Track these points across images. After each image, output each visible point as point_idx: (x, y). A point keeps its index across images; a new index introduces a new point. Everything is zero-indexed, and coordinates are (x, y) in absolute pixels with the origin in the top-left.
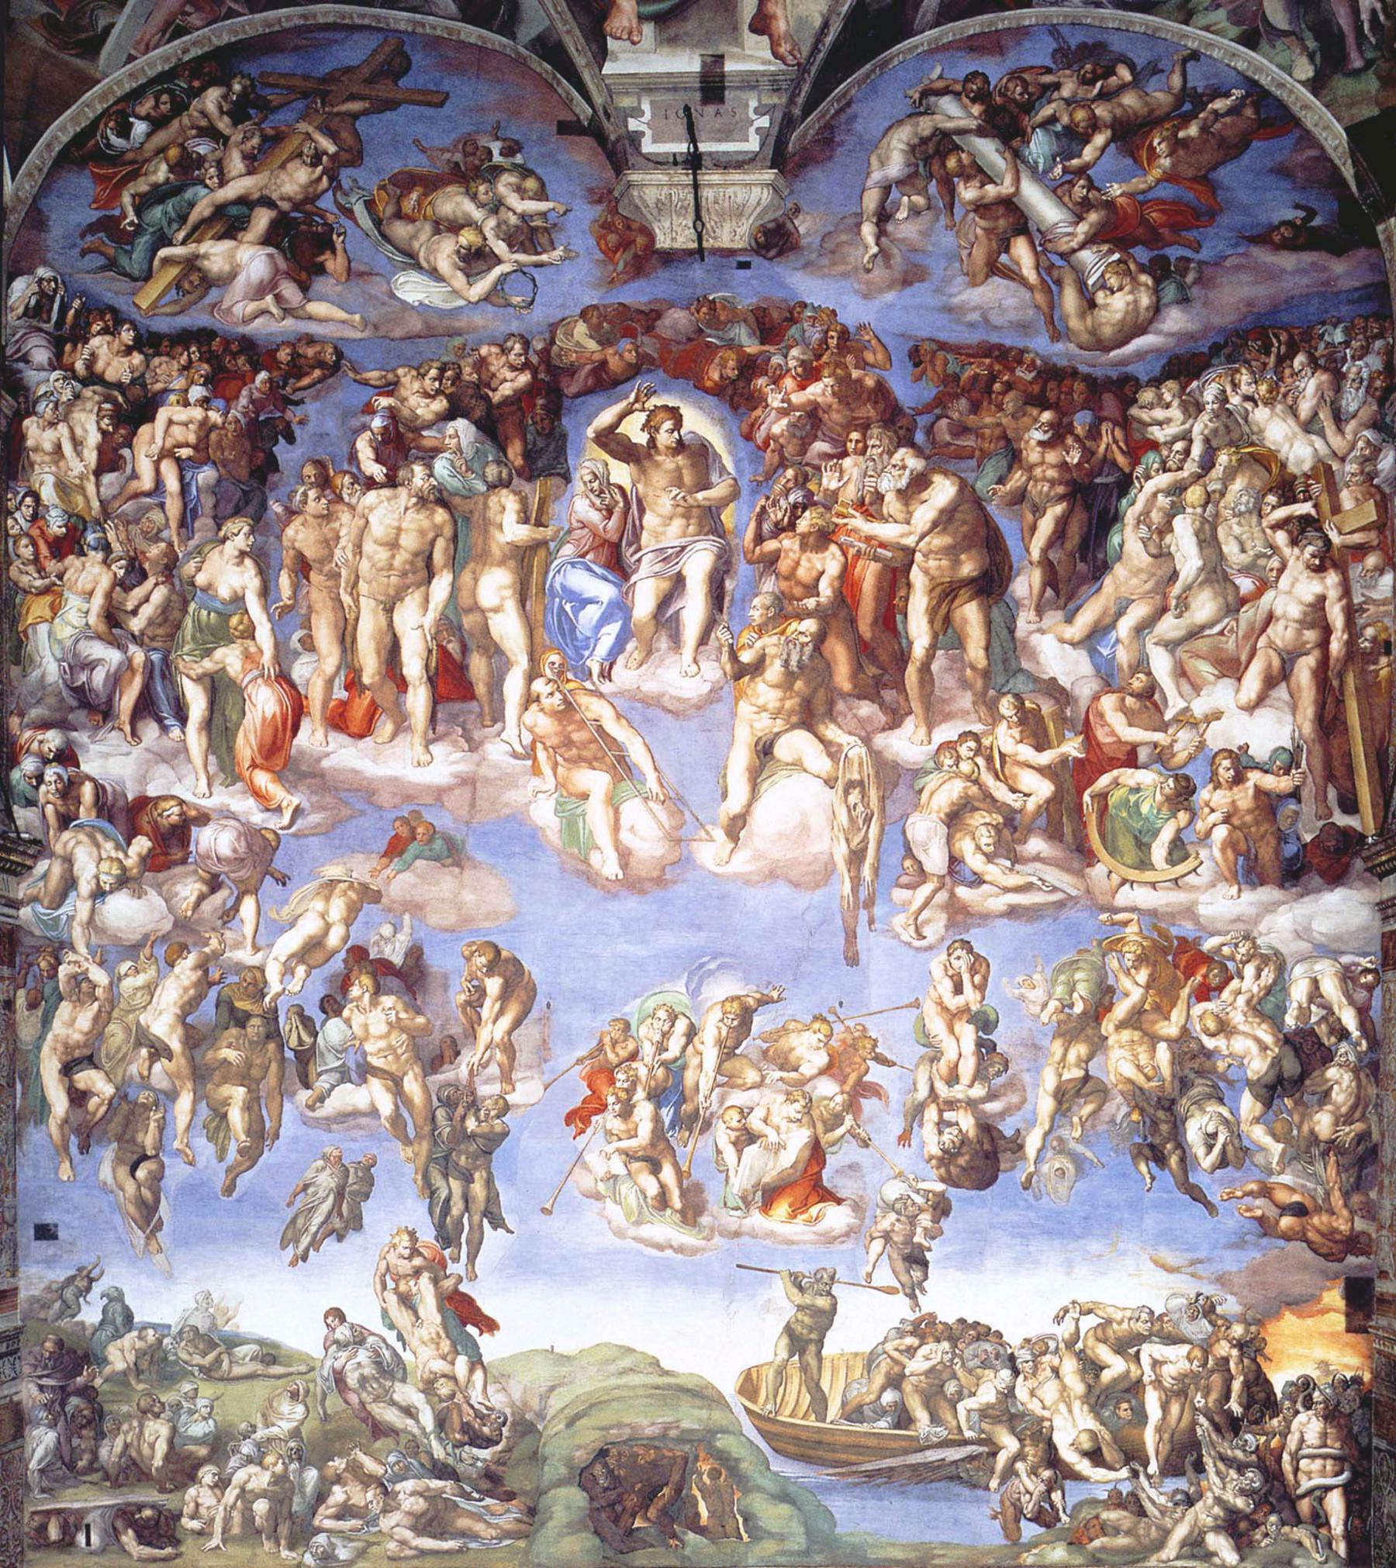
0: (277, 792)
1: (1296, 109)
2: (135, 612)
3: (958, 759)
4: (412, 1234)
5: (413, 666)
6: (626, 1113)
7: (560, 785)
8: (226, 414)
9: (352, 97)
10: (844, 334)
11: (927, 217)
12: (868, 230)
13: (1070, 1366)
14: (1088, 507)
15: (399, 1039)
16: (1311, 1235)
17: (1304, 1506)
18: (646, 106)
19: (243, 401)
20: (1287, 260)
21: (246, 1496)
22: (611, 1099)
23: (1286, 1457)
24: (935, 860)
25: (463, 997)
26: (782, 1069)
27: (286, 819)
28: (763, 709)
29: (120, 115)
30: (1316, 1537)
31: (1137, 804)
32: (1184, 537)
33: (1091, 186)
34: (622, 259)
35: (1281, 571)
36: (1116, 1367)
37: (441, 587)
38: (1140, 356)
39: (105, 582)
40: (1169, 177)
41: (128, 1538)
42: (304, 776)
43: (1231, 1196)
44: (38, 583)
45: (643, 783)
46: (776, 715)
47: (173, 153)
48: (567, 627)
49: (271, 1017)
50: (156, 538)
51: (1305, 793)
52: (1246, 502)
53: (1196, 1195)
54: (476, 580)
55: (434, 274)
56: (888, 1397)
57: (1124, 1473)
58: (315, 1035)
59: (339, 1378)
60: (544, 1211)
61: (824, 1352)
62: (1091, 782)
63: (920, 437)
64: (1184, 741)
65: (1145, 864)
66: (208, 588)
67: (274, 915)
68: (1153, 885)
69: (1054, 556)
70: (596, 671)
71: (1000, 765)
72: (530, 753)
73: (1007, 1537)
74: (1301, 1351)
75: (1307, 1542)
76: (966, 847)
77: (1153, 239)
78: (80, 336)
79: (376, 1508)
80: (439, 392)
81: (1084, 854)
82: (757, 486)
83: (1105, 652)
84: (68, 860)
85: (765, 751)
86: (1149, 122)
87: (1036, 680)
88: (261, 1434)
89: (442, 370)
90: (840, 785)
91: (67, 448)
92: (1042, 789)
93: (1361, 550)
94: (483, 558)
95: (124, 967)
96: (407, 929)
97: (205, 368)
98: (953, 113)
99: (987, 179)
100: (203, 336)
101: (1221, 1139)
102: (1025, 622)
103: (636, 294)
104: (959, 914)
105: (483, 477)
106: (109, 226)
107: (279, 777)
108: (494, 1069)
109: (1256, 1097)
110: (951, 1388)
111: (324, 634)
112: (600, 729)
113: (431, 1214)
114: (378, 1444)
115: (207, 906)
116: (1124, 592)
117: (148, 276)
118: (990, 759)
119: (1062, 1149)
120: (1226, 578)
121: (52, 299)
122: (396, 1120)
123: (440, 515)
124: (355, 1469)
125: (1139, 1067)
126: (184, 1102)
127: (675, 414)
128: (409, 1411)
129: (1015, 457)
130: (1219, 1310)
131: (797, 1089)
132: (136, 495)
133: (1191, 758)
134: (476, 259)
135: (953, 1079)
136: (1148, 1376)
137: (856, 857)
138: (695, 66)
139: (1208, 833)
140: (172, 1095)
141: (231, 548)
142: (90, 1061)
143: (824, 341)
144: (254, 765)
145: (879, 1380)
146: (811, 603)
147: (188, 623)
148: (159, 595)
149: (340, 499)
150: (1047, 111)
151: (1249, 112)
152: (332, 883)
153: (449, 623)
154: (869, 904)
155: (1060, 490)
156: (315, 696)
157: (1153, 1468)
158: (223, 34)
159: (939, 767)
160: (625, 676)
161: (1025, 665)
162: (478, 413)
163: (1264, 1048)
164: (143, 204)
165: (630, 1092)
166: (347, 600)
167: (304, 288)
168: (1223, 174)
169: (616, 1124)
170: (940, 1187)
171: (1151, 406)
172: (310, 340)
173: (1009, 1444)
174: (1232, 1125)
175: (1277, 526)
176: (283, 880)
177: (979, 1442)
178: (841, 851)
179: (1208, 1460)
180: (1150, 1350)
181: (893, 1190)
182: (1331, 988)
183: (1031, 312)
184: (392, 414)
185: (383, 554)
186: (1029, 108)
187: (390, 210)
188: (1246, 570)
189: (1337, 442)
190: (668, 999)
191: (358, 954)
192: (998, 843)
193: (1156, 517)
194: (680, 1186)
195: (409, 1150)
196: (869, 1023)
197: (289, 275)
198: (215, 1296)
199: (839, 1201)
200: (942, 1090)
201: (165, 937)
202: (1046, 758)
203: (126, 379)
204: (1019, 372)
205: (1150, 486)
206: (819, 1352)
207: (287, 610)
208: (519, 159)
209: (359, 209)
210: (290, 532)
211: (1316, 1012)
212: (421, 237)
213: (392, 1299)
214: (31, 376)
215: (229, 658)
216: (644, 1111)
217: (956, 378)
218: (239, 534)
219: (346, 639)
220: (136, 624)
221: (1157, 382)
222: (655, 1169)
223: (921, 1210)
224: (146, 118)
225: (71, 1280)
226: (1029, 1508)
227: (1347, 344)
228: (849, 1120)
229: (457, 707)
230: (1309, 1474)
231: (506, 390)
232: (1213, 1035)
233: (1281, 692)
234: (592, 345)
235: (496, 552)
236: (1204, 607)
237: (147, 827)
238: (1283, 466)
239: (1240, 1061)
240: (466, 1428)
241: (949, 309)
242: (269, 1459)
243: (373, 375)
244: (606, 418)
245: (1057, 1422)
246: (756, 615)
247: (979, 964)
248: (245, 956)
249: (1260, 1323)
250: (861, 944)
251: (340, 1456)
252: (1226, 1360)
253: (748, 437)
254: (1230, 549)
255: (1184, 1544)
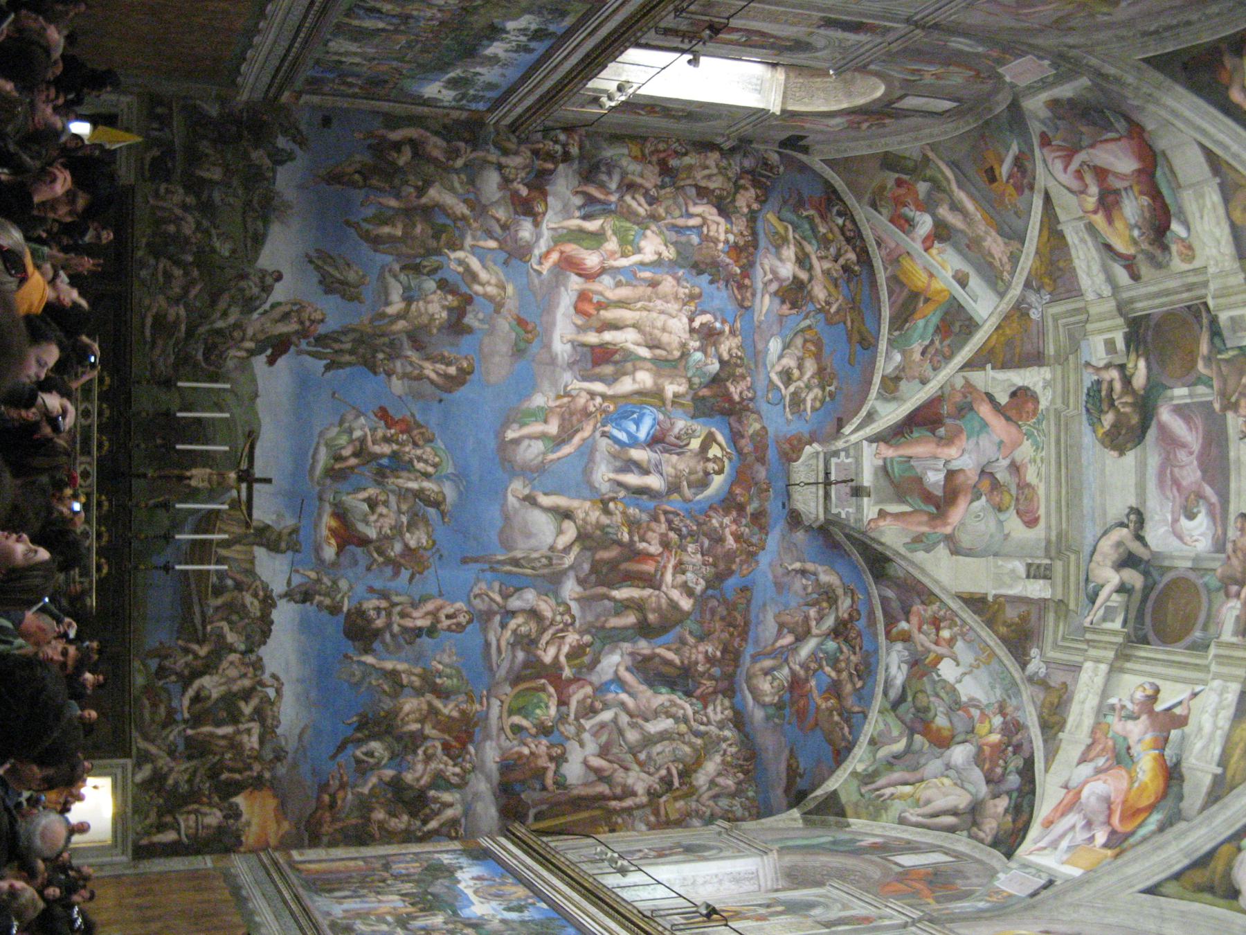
0: (547, 265)
1: (844, 765)
2: (633, 198)
3: (562, 614)
4: (322, 321)
5: (608, 336)
6: (387, 440)
7: (551, 409)
8: (723, 252)
9: (853, 321)
10: (753, 555)
11: (801, 593)
12: (797, 565)
13: (247, 683)
14: (678, 676)
15: (425, 320)
16: (320, 812)
17: (168, 819)
18: (849, 460)
19: (728, 260)
20: (783, 767)
21: (177, 220)
22: (393, 431)
23: (195, 806)
24: (515, 603)
25: (446, 354)
26: (409, 522)
27: (536, 267)
28: (587, 514)
29: (846, 213)
30: (151, 826)
31: (539, 707)
32: (665, 724)
33: (815, 671)
34: (787, 447)
35: (649, 773)
36: (247, 709)
37: (644, 352)
38: (744, 698)
39: (648, 185)
40: (818, 708)
41: (156, 152)
42: (557, 276)
43: (340, 767)
44: (647, 151)
45: (553, 452)
46: (584, 520)
47: (830, 236)
48: (626, 416)
49: (438, 252)
50: (667, 212)
51: (545, 793)
52: (679, 754)
53: (342, 747)
54: (647, 370)
55: (781, 357)
56: (230, 582)
57: (187, 715)
58: (428, 274)
59: (244, 276)
60: (334, 394)
61: (256, 548)
62: (551, 683)
63: (710, 592)
64: (570, 730)
65: (511, 712)
66: (644, 236)
67: (489, 256)
68: (500, 718)
69: (657, 660)
70: (606, 429)
71: (558, 638)
72: (567, 394)
73: (150, 651)
74: (256, 809)
75: (147, 822)
76: (520, 620)
77: (793, 703)
78: (756, 184)
79: (170, 293)
80: (731, 356)
81: (516, 680)
82: (689, 512)
83: (612, 688)
84: (516, 153)
85: (567, 515)
86: (839, 697)
87: (600, 653)
88: (213, 232)
89: (740, 358)
90: (550, 554)
91: (707, 172)
92: (548, 658)
93: (656, 813)
94: (657, 375)
95: (463, 177)
96: (481, 326)
97: (741, 243)
98: (845, 604)
99: (820, 619)
100: (755, 244)
101: (371, 760)
102: (627, 646)
103: (772, 454)
104: (486, 616)
105: (694, 376)
106: (801, 203)
107: (557, 265)
108: (409, 369)
109: (393, 778)
110: (235, 618)
111: (623, 292)
112: (577, 431)
113: (333, 332)
114: (206, 296)
115: (493, 223)
116: (640, 695)
117: (781, 220)
118: (562, 631)
119: (365, 676)
120: (645, 746)
121: (771, 170)
122: (383, 315)
123: (677, 354)
124: (192, 283)
125: (407, 715)
126: (393, 203)
127: (720, 472)
128: (225, 314)
129: (701, 639)
130: (279, 764)
131: (398, 530)
132: (686, 204)
133: (562, 733)
134: (787, 376)
135: (403, 615)
136: (242, 727)
137: (516, 562)
138: (866, 484)
139: (525, 745)
140: (398, 197)
141: (662, 249)
142: (416, 154)
143: (752, 545)
144: (562, 253)
145: (238, 577)
146: (636, 538)
147: (628, 225)
148: (641, 211)
149: (685, 304)
150: (845, 649)
151: (843, 744)
152: (504, 288)
153: (629, 356)
154: (493, 569)
155: (686, 662)
156: (594, 286)
157: (190, 732)
158: (878, 263)
159: (558, 604)
160: (604, 443)
161: (607, 647)
162: (722, 375)
163: (418, 780)
164: (810, 219)
165: (397, 442)
166: (639, 305)
167: (776, 294)
168: (818, 732)
169: (380, 433)
170: (345, 609)
171: (722, 704)
172: (754, 295)
173: (203, 651)
174: (378, 765)
175: (668, 770)
176: (506, 263)
177: (204, 634)
178: (519, 554)
179: (194, 763)
180: (256, 728)
181: (343, 584)
182: (449, 813)
183: (763, 645)
184: (721, 333)
185: (659, 324)
186: (846, 640)
187: (808, 337)
188: (649, 757)
189: (706, 796)
190: (444, 464)
191: (468, 300)
192: (523, 636)
193: (674, 710)
194: (348, 468)
195: (366, 322)
196: (432, 570)
197: (781, 286)
198: (289, 212)
199: (338, 554)
200: (399, 608)
201: (477, 199)
202: (562, 659)
203: (737, 204)
204: (738, 640)
205: (687, 706)
206: (254, 544)
207: (635, 274)
208: (828, 399)
209: (808, 322)
210: (670, 279)
211: (436, 807)
212: (796, 350)
213: (287, 309)
214: (738, 157)
215: (612, 244)
216: (386, 449)
217: (735, 609)
218: (669, 254)
219: (622, 304)
220: (628, 198)
221: (732, 708)
222: (355, 455)
223: (333, 599)
224: (844, 225)
225: (300, 132)
226: (167, 663)
227: (747, 799)
228: (381, 559)
229: (589, 356)
230: (187, 820)
231: (732, 389)
232: (425, 752)
233: (593, 777)
234: (751, 431)
235: (660, 381)
236: (632, 736)
237: (533, 195)
238: (695, 771)
239: (411, 768)
240: (215, 346)
241: (764, 605)
242: (199, 235)
243: (738, 325)
244: (720, 437)
245: (216, 678)
246: (631, 511)
247: (460, 628)
248: (469, 241)
249: (272, 788)
250: (472, 565)
251: (201, 274)
252: (250, 768)
253: (711, 507)
254: (659, 748)
255: (147, 751)
